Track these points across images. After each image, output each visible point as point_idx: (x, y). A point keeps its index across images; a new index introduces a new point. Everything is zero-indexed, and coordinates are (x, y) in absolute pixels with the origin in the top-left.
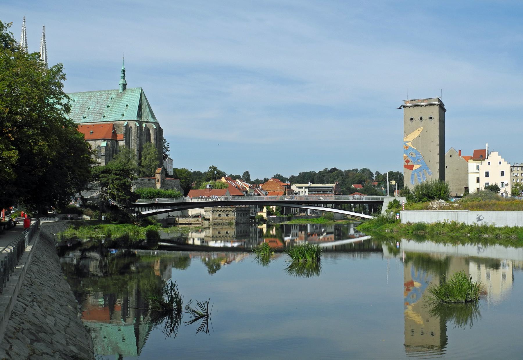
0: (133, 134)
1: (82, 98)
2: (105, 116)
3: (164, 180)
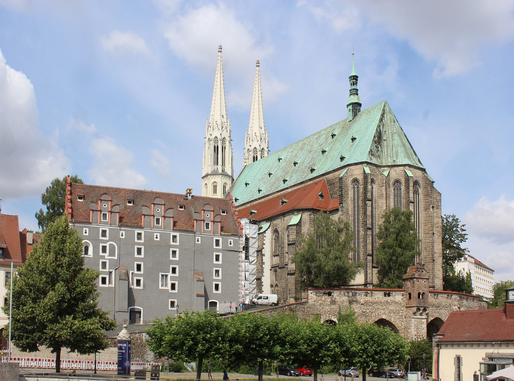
0: (360, 194)
1: (292, 152)
2: (314, 170)
3: (423, 293)
